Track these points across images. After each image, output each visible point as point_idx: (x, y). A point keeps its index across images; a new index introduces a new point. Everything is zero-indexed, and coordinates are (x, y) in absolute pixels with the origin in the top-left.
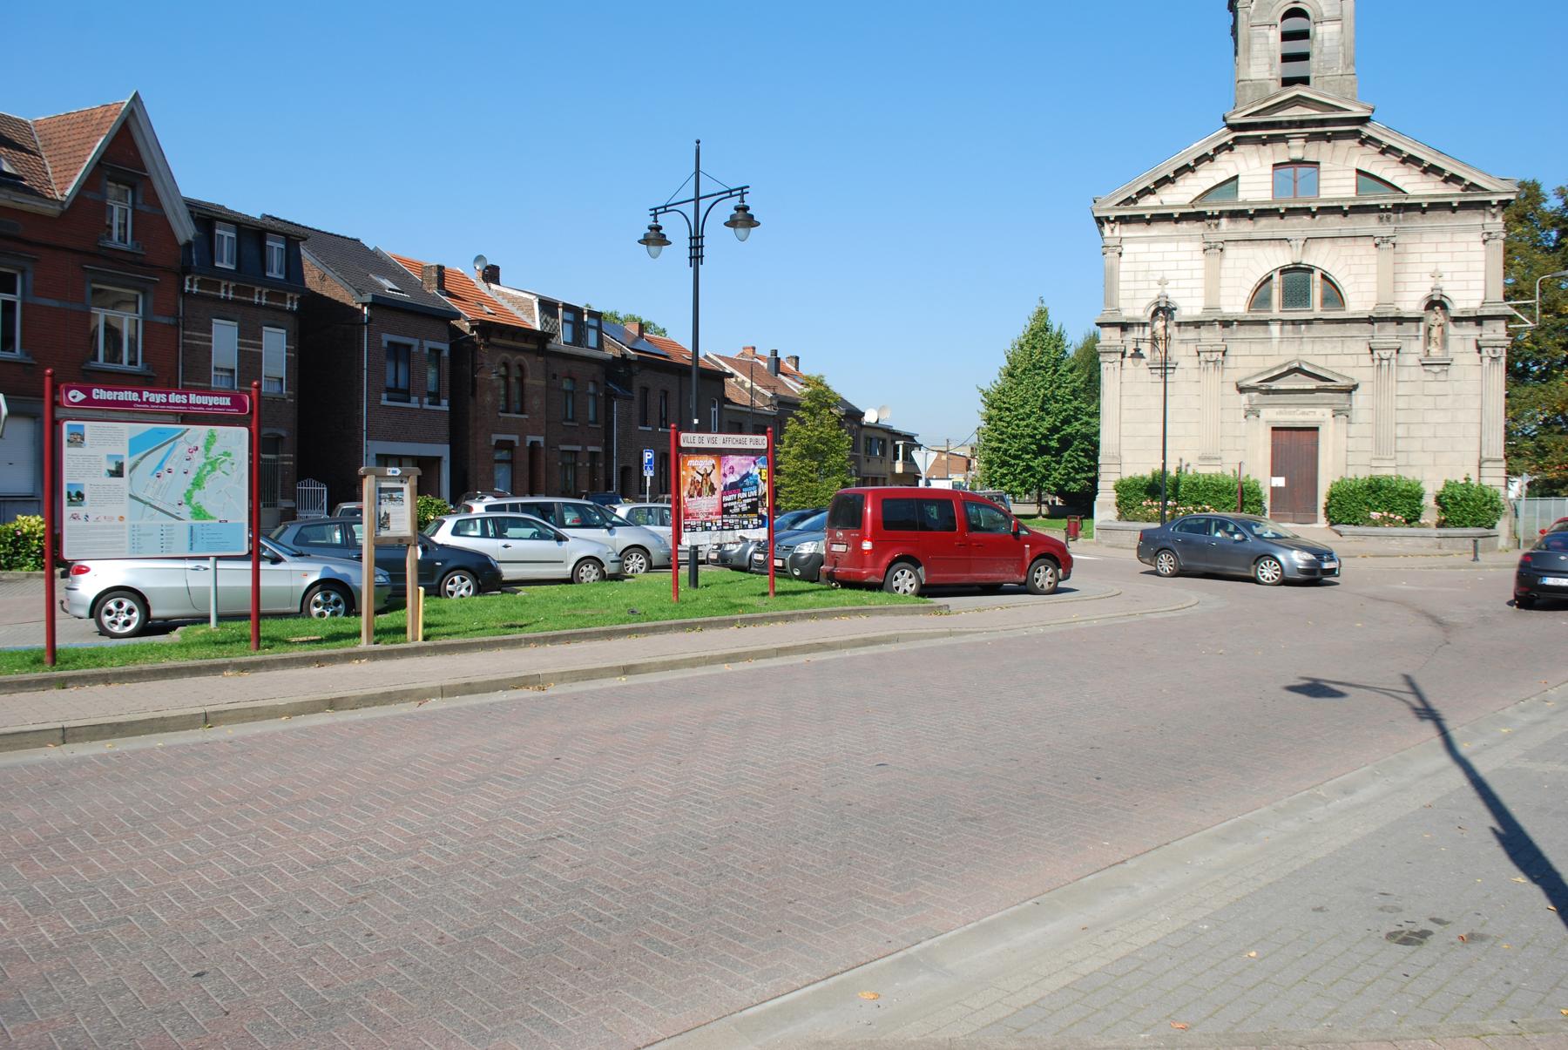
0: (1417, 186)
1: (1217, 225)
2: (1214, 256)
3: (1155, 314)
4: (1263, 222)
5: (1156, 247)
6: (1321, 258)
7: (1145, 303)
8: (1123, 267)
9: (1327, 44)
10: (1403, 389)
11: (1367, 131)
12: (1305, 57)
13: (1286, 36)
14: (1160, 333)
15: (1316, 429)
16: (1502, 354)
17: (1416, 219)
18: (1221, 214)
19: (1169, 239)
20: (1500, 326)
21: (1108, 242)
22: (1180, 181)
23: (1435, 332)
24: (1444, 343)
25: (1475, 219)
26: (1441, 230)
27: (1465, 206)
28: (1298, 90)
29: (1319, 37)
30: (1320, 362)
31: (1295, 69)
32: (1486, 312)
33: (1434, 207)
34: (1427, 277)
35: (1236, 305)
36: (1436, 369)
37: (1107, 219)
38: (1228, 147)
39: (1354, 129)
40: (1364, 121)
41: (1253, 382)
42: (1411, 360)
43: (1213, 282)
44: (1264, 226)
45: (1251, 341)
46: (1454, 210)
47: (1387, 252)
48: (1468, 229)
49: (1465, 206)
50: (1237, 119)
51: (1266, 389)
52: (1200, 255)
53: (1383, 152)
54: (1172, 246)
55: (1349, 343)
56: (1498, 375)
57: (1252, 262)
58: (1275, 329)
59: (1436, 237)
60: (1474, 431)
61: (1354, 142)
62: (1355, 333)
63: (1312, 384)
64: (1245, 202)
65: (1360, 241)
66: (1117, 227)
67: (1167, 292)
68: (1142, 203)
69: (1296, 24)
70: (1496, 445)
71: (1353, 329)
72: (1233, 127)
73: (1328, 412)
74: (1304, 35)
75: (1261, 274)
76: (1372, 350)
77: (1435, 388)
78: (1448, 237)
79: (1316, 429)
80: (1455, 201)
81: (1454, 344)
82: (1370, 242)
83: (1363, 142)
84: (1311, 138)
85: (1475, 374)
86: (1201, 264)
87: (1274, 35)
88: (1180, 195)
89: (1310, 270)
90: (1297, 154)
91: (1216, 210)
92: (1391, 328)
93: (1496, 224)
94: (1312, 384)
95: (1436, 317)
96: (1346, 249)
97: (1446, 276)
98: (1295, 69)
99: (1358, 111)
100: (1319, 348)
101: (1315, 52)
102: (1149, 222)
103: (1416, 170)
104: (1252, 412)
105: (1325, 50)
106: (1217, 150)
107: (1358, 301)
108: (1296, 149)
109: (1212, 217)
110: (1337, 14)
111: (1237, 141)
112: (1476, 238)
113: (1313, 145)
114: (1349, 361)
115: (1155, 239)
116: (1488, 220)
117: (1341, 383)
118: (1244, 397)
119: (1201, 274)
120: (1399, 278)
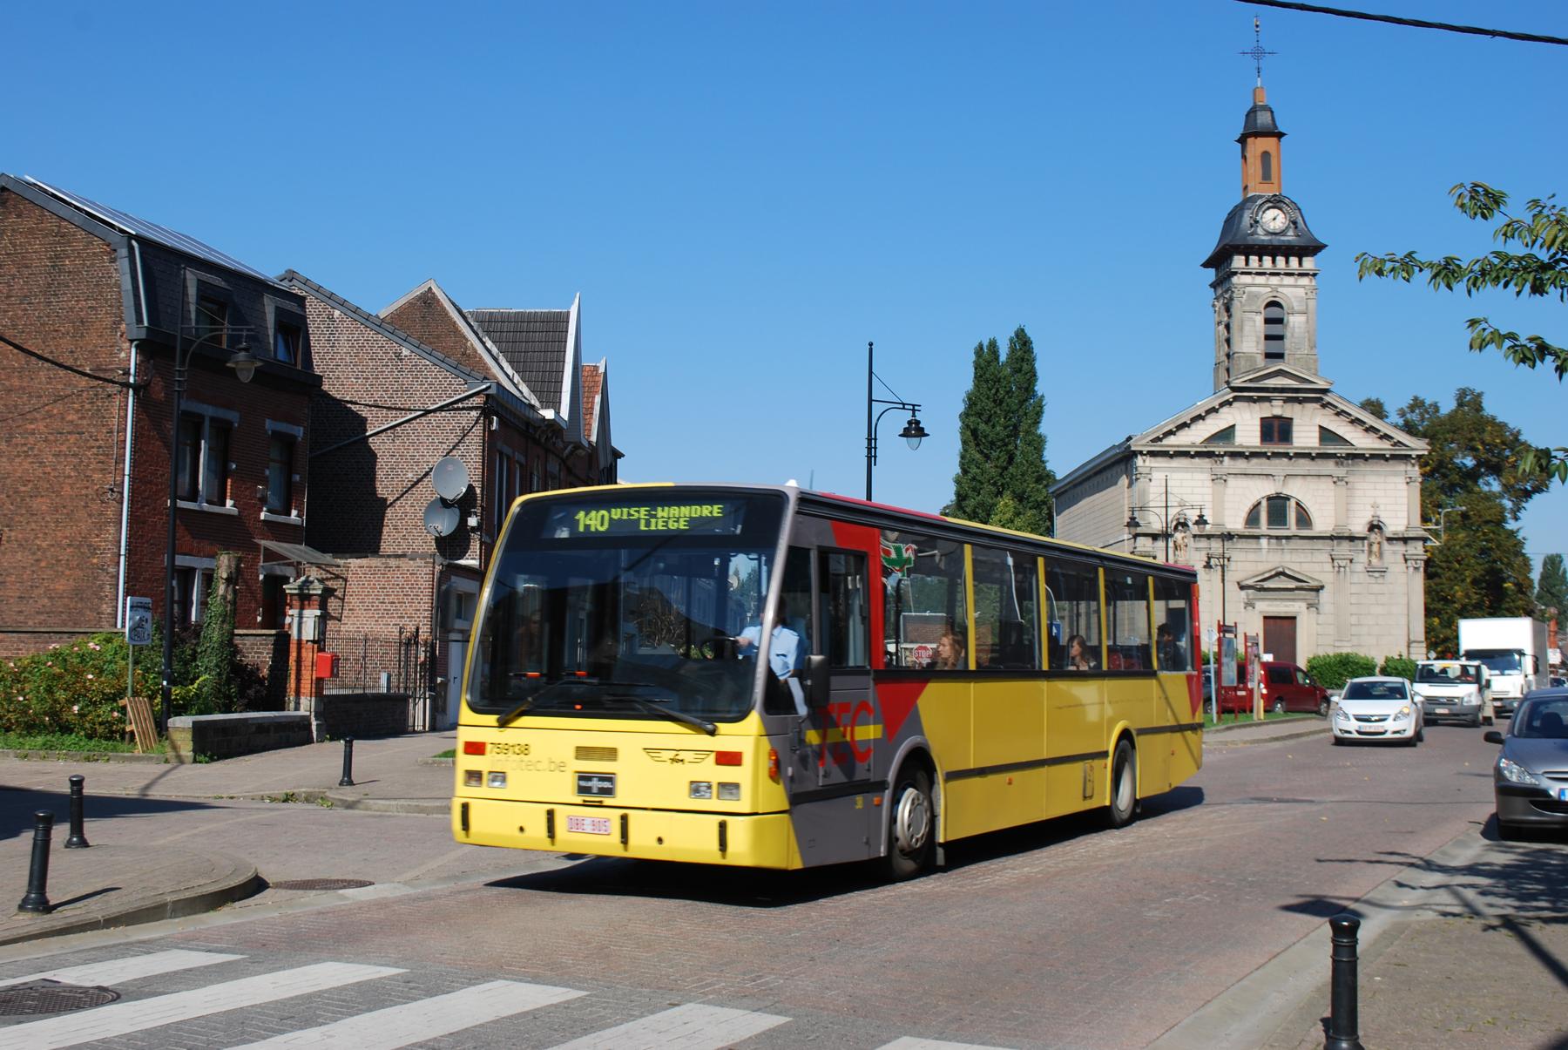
0: (1361, 441)
4: (1254, 461)
8: (1152, 490)
10: (1354, 589)
11: (1327, 399)
12: (1281, 338)
13: (1268, 321)
14: (1180, 541)
15: (1294, 618)
16: (1422, 564)
17: (1362, 467)
18: (1226, 454)
19: (1186, 470)
20: (1420, 543)
22: (1193, 427)
23: (1375, 548)
24: (1381, 555)
25: (1401, 467)
26: (1377, 473)
27: (1394, 457)
31: (1274, 347)
32: (1411, 535)
33: (1373, 456)
35: (1236, 523)
37: (1141, 453)
38: (1228, 403)
39: (1318, 397)
40: (1325, 391)
41: (1250, 582)
42: (1359, 567)
43: (1219, 503)
44: (1255, 465)
45: (1246, 550)
46: (1387, 460)
48: (1395, 474)
49: (1394, 457)
50: (1237, 383)
51: (1258, 588)
52: (1210, 483)
53: (1338, 414)
54: (1188, 476)
55: (1317, 554)
56: (1418, 581)
58: (1264, 542)
59: (1373, 478)
60: (1404, 621)
61: (1317, 406)
63: (1293, 585)
66: (1148, 459)
68: (1165, 442)
69: (1274, 312)
70: (1419, 631)
71: (1319, 544)
72: (1234, 389)
73: (1303, 605)
74: (1280, 321)
75: (1254, 501)
77: (1376, 588)
78: (1382, 479)
79: (1294, 618)
80: (1388, 454)
82: (1330, 480)
83: (1324, 406)
84: (1287, 400)
85: (1403, 579)
86: (1209, 491)
87: (1260, 319)
88: (1195, 436)
89: (1288, 498)
90: (1277, 411)
91: (1222, 450)
92: (1346, 545)
93: (1415, 471)
94: (1293, 585)
95: (1374, 537)
96: (1312, 484)
98: (1274, 347)
99: (1322, 385)
100: (1295, 557)
101: (1288, 335)
102: (1171, 457)
103: (1360, 428)
104: (1249, 604)
106: (1222, 405)
107: (1322, 523)
108: (1277, 409)
110: (1303, 308)
111: (1236, 399)
112: (1401, 480)
113: (1289, 406)
114: (1317, 567)
116: (1409, 468)
117: (1313, 584)
118: (1243, 593)
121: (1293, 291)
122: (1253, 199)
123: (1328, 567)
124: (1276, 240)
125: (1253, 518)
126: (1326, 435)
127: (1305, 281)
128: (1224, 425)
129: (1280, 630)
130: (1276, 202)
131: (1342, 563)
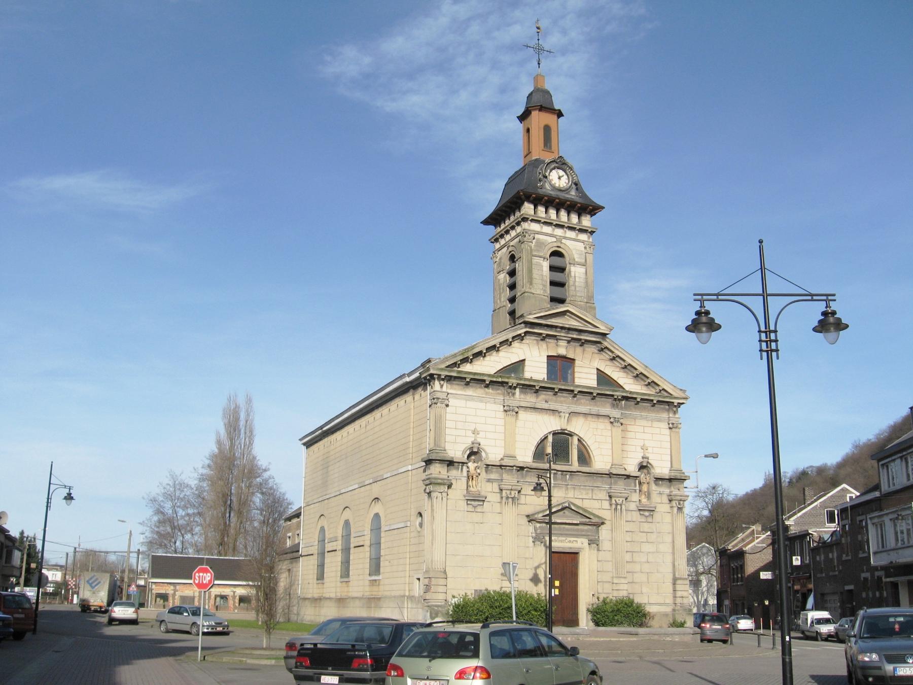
1: (514, 394)
2: (511, 419)
3: (469, 457)
4: (543, 396)
5: (470, 404)
6: (578, 427)
7: (463, 447)
8: (448, 416)
9: (577, 279)
10: (630, 526)
12: (562, 285)
13: (552, 268)
21: (438, 395)
23: (645, 488)
24: (649, 496)
26: (646, 418)
28: (562, 308)
29: (573, 274)
30: (578, 503)
31: (558, 292)
34: (639, 449)
36: (647, 513)
38: (520, 338)
39: (597, 340)
40: (604, 335)
42: (633, 506)
43: (510, 437)
47: (617, 430)
48: (659, 420)
52: (502, 415)
54: (482, 405)
55: (596, 491)
57: (534, 427)
59: (644, 423)
60: (669, 559)
62: (599, 484)
64: (531, 379)
65: (601, 420)
67: (479, 440)
69: (557, 261)
73: (586, 542)
75: (541, 435)
76: (610, 497)
77: (646, 527)
78: (649, 424)
79: (577, 553)
80: (655, 400)
81: (655, 498)
82: (607, 421)
85: (668, 519)
86: (502, 422)
87: (546, 265)
88: (489, 366)
89: (571, 434)
90: (562, 351)
97: (650, 450)
98: (558, 292)
99: (603, 329)
100: (578, 494)
105: (577, 284)
107: (601, 461)
108: (562, 349)
109: (510, 387)
115: (469, 398)
117: (595, 520)
119: (502, 429)
120: (625, 448)
121: (575, 246)
122: (538, 162)
123: (606, 504)
124: (563, 195)
125: (539, 454)
126: (603, 378)
127: (584, 237)
128: (515, 359)
129: (564, 566)
130: (561, 164)
131: (619, 501)
